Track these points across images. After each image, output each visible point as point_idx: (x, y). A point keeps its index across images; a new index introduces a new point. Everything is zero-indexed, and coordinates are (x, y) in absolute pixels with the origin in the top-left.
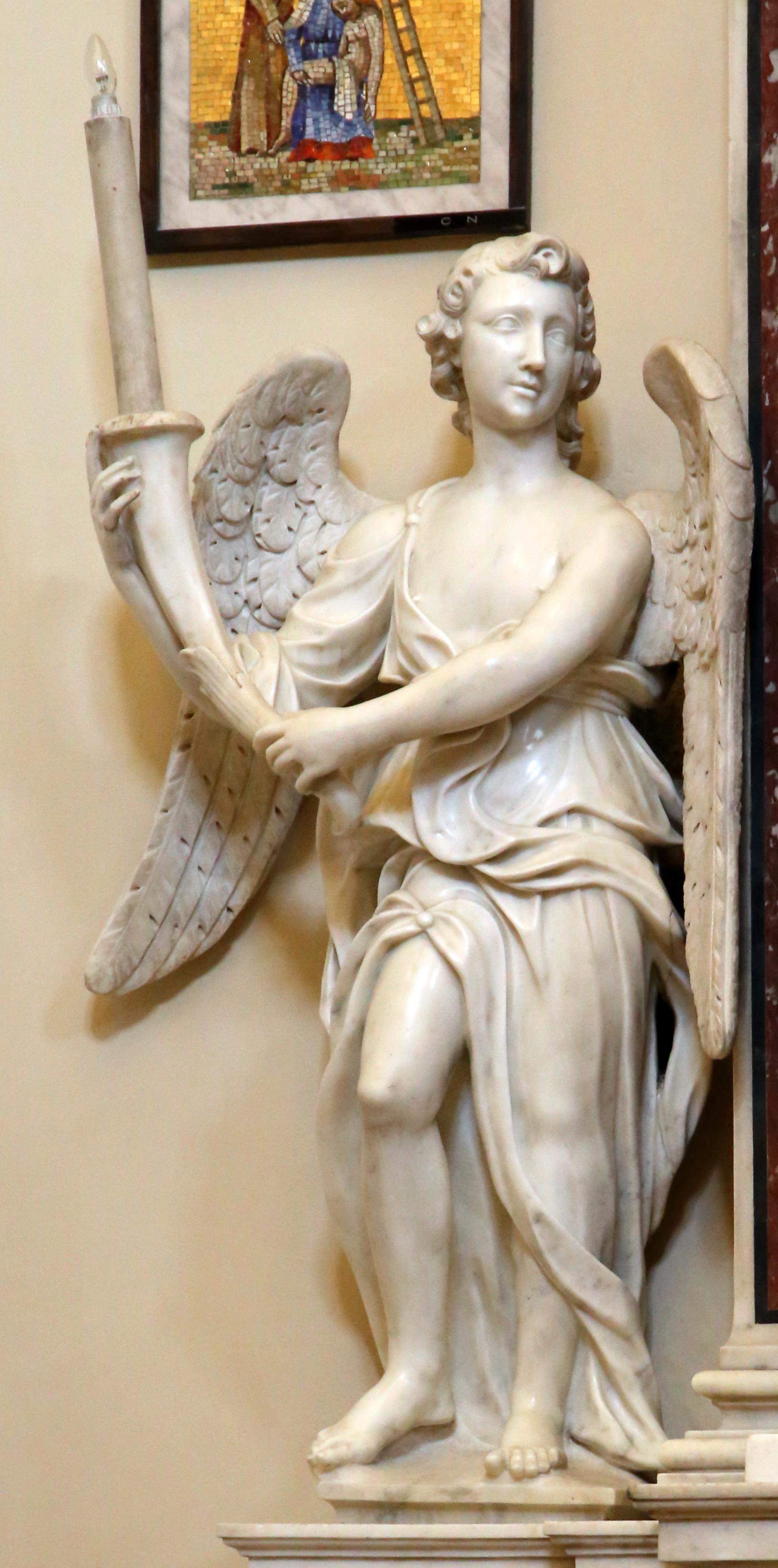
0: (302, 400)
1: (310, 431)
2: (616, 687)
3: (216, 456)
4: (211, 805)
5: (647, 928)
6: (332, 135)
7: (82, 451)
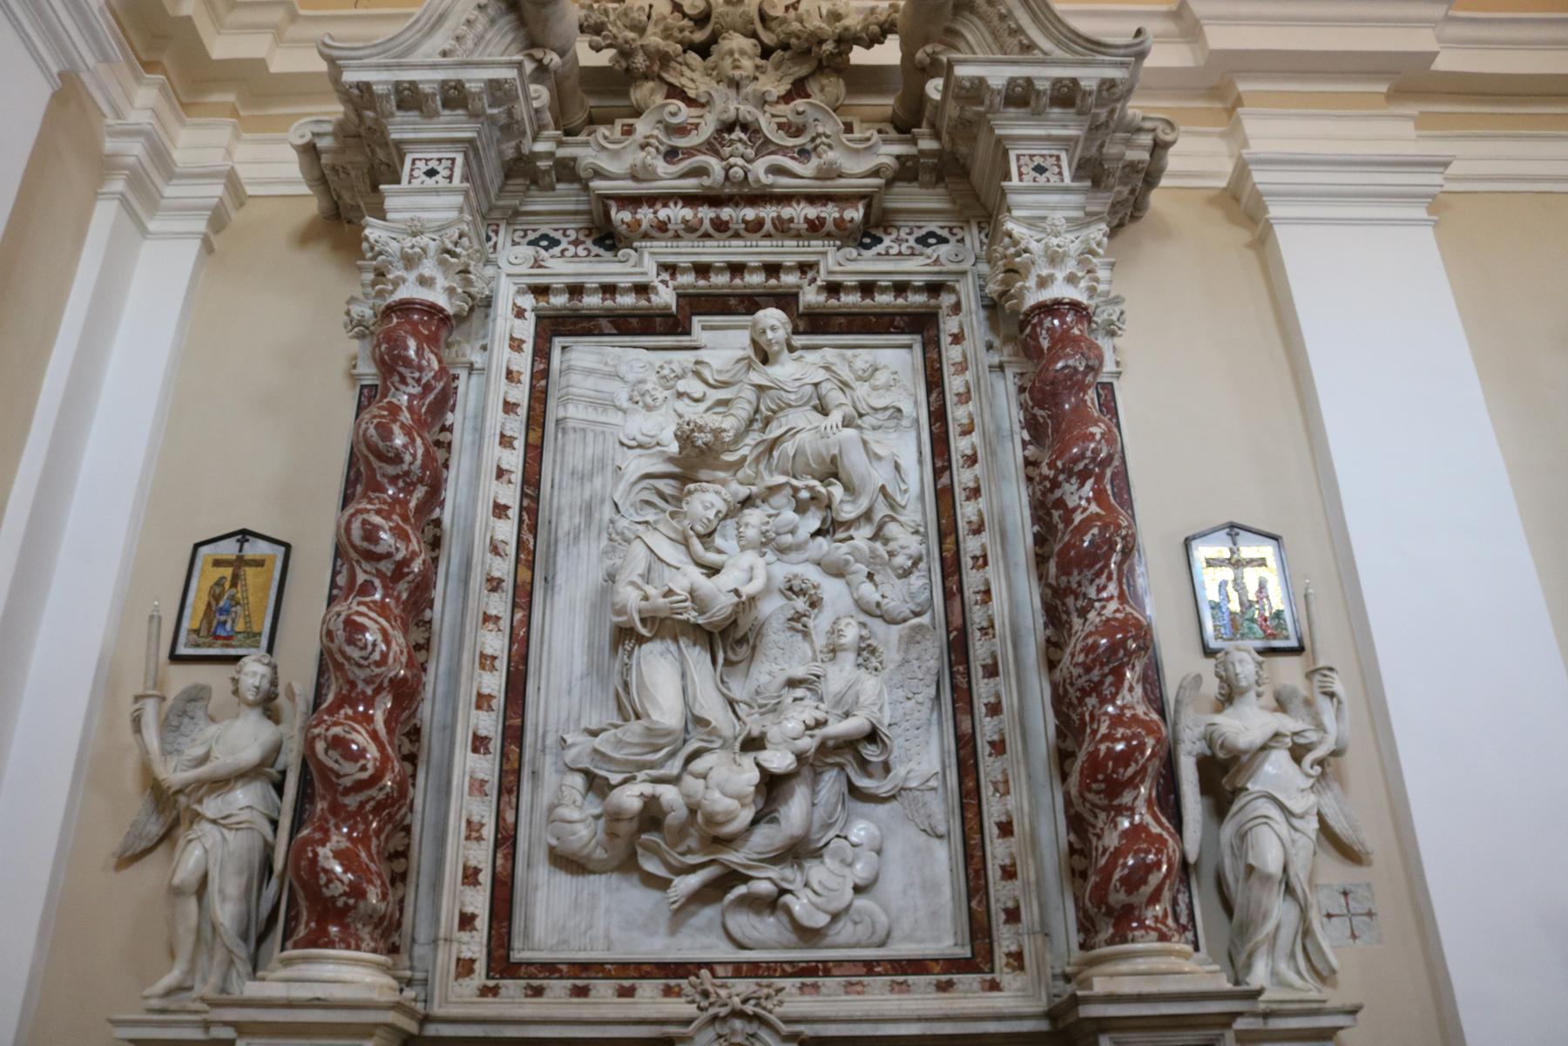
0: (197, 695)
1: (200, 704)
2: (268, 776)
3: (172, 707)
4: (157, 805)
5: (266, 841)
6: (223, 634)
7: (130, 699)
